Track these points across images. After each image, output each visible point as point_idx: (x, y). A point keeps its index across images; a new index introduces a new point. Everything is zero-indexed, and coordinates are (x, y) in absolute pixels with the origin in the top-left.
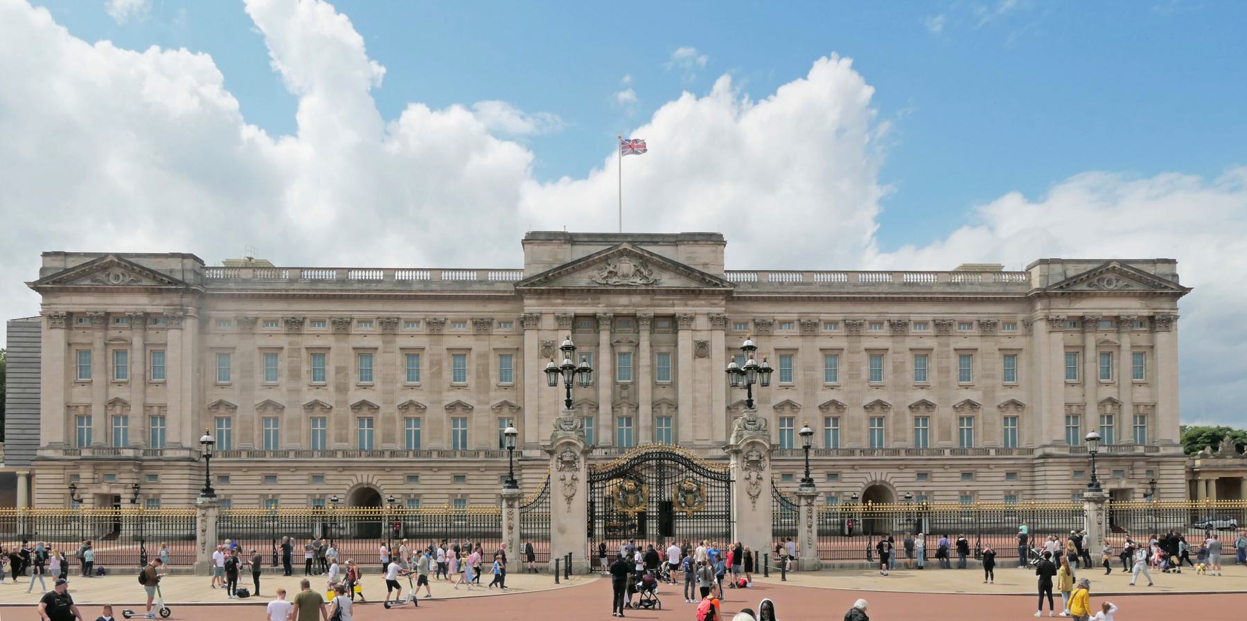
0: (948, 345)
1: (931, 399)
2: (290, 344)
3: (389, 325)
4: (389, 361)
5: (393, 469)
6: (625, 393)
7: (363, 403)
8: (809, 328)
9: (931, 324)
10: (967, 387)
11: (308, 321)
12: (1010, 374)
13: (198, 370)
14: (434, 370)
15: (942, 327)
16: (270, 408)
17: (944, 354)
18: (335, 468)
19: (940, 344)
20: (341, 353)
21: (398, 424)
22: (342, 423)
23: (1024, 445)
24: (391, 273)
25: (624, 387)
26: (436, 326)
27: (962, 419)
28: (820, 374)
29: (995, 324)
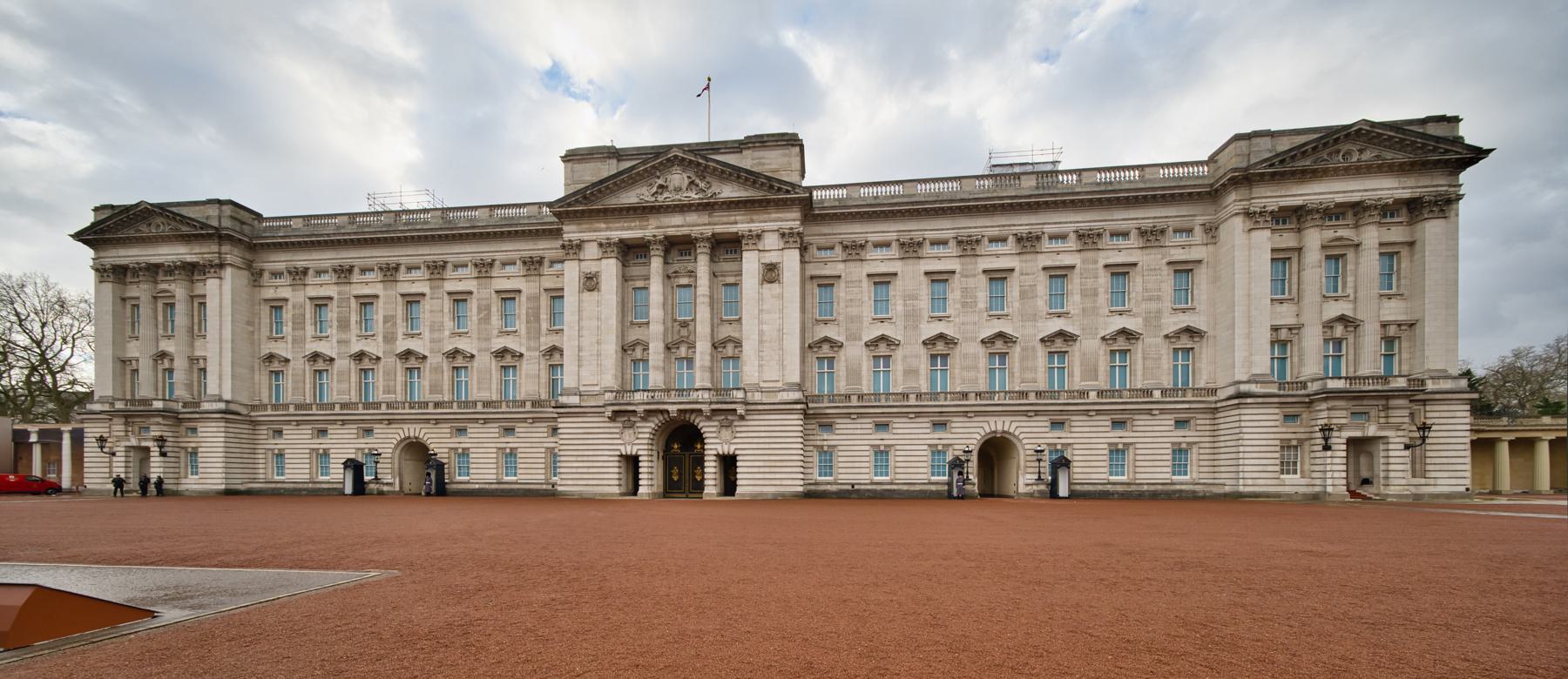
0: (1096, 262)
1: (1070, 329)
4: (435, 309)
6: (684, 332)
8: (911, 249)
9: (1073, 236)
12: (1184, 294)
13: (249, 323)
15: (1088, 239)
17: (1090, 270)
19: (1083, 262)
20: (388, 301)
23: (1202, 385)
25: (684, 324)
27: (1113, 352)
28: (924, 304)
29: (1163, 232)
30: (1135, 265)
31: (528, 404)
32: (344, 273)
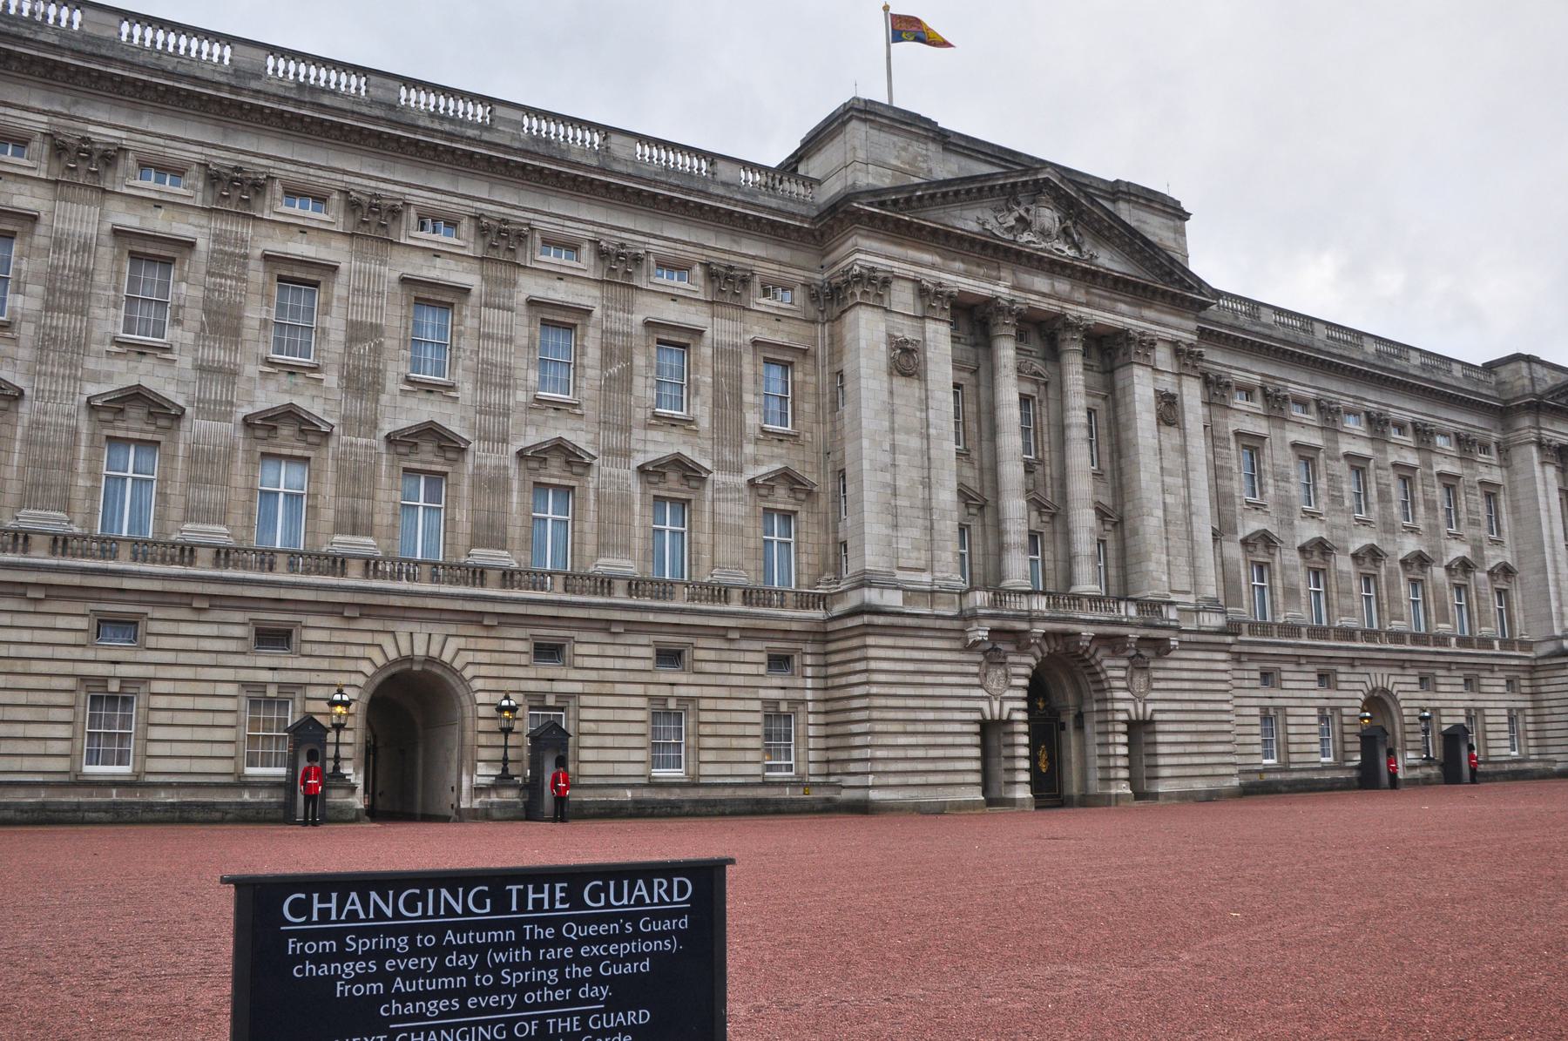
0: (1431, 467)
2: (218, 238)
3: (503, 242)
5: (506, 619)
7: (431, 432)
8: (1276, 404)
9: (1409, 426)
10: (1457, 537)
11: (278, 187)
14: (614, 370)
15: (1424, 435)
16: (135, 413)
18: (335, 609)
21: (515, 498)
22: (355, 477)
24: (514, 115)
26: (619, 266)
28: (1295, 490)
29: (1474, 442)
30: (1458, 477)
31: (736, 594)
32: (235, 190)
